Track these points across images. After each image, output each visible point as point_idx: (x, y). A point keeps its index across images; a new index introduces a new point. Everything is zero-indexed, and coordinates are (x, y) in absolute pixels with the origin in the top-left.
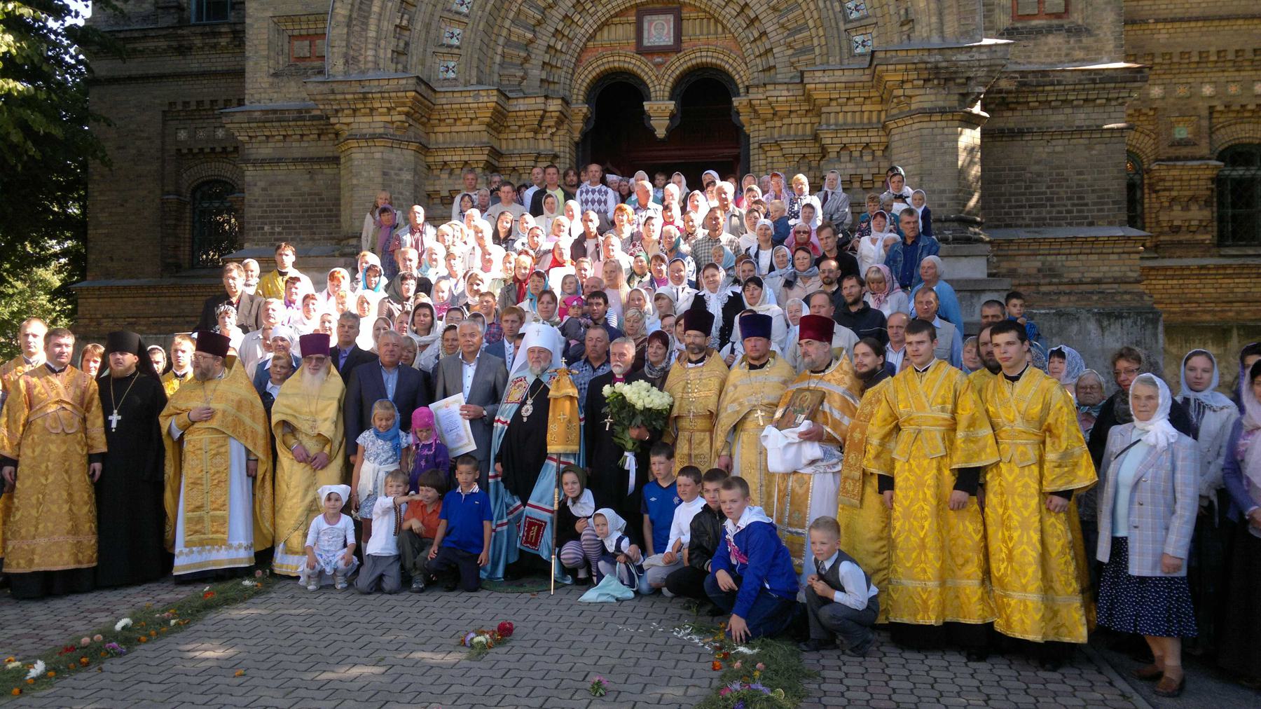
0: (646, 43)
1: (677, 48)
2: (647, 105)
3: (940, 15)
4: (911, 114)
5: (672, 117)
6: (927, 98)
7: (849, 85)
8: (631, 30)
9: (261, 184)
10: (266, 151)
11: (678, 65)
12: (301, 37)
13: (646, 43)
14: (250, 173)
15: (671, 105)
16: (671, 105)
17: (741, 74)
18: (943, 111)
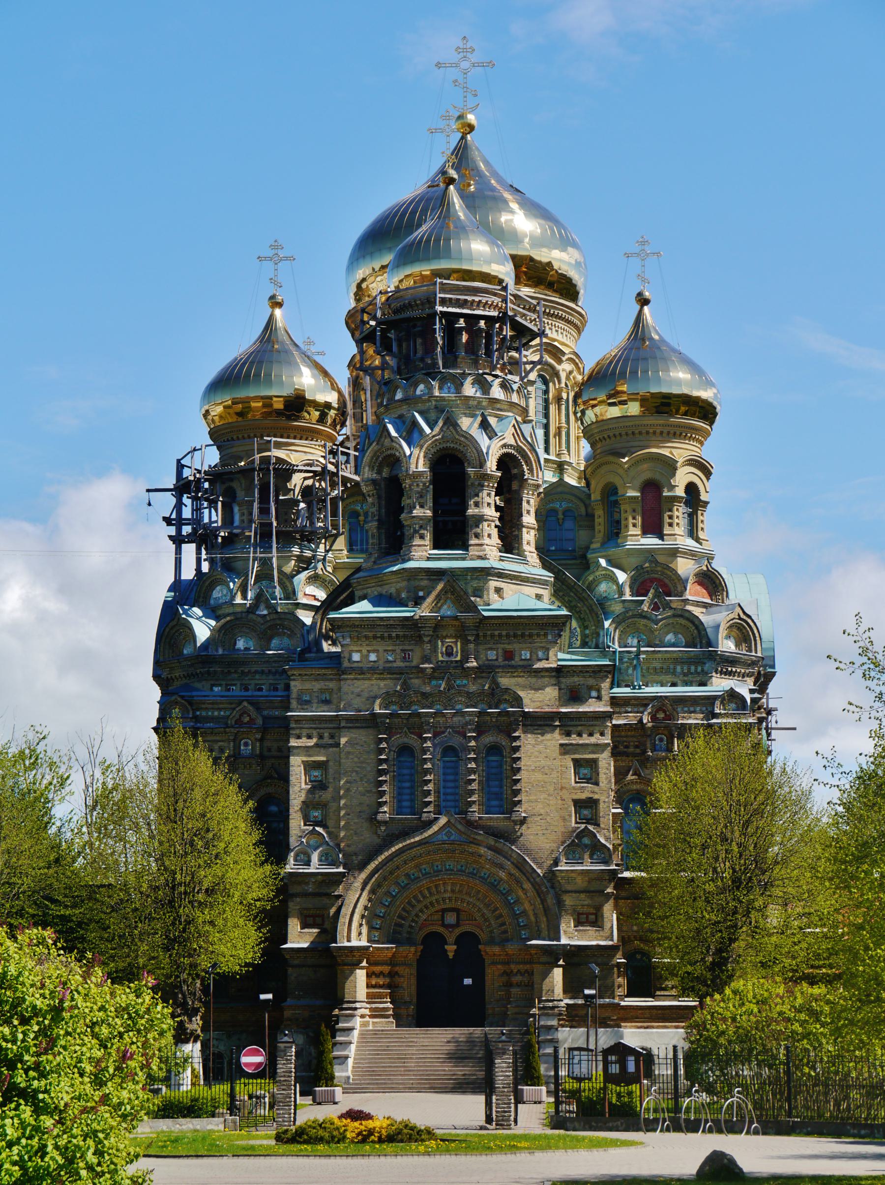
0: (446, 923)
1: (458, 925)
2: (446, 947)
3: (548, 931)
4: (539, 963)
5: (456, 951)
6: (544, 959)
7: (520, 950)
8: (440, 917)
9: (295, 975)
10: (296, 962)
11: (458, 931)
12: (309, 916)
13: (446, 923)
14: (290, 970)
15: (455, 947)
16: (455, 947)
17: (483, 936)
18: (548, 963)
